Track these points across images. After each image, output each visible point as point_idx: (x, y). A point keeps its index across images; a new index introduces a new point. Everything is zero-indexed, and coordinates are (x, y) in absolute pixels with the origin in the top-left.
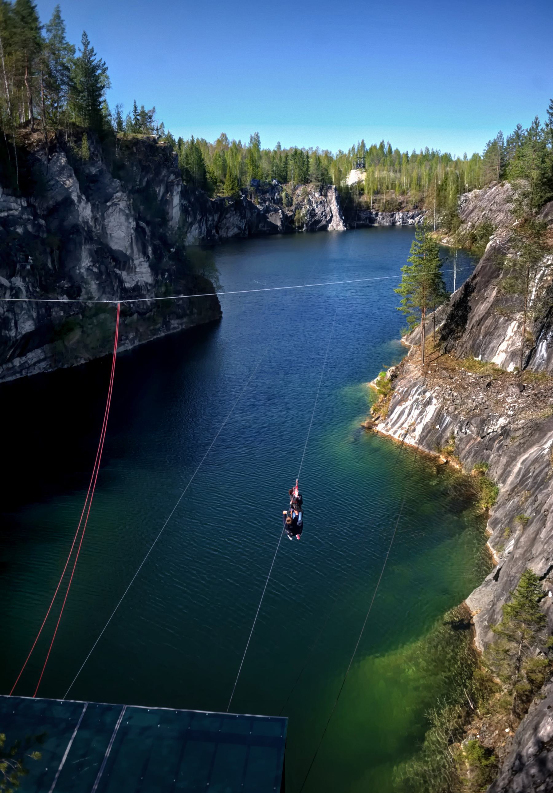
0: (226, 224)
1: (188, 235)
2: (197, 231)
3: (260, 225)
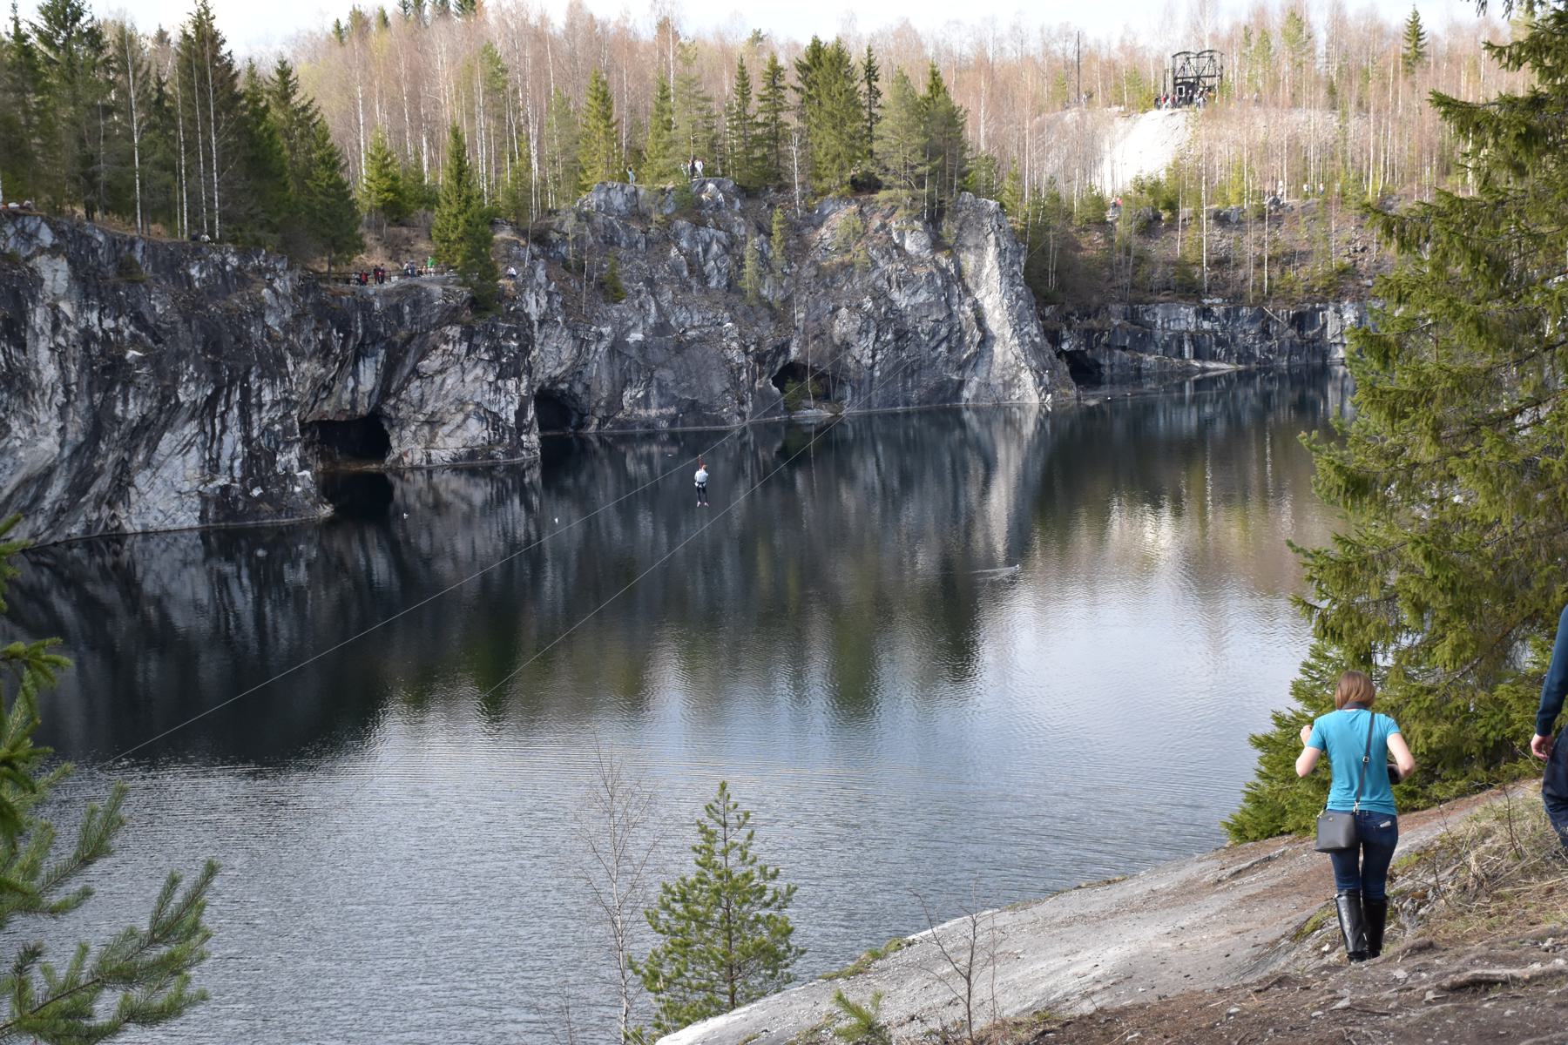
0: (422, 401)
1: (140, 480)
2: (194, 457)
3: (628, 394)
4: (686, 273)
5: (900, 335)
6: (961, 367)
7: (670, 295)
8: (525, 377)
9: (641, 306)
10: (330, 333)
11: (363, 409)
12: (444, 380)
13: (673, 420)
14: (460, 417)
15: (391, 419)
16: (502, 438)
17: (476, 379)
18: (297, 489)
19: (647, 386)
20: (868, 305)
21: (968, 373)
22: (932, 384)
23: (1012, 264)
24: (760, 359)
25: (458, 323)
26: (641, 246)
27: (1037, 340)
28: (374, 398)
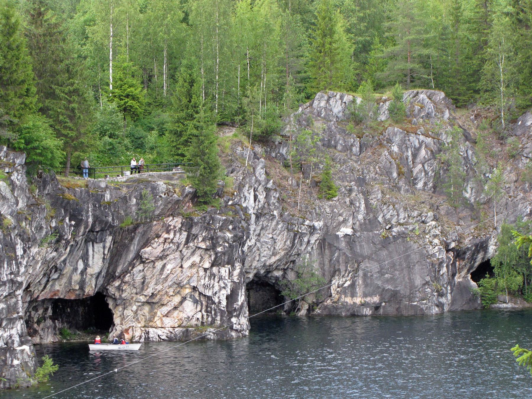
3: (335, 282)
4: (395, 175)
8: (238, 265)
9: (352, 203)
10: (63, 220)
11: (90, 290)
12: (164, 266)
13: (377, 308)
14: (177, 299)
15: (115, 299)
16: (214, 320)
17: (193, 265)
18: (16, 362)
24: (459, 254)
25: (179, 214)
26: (356, 149)
28: (101, 281)
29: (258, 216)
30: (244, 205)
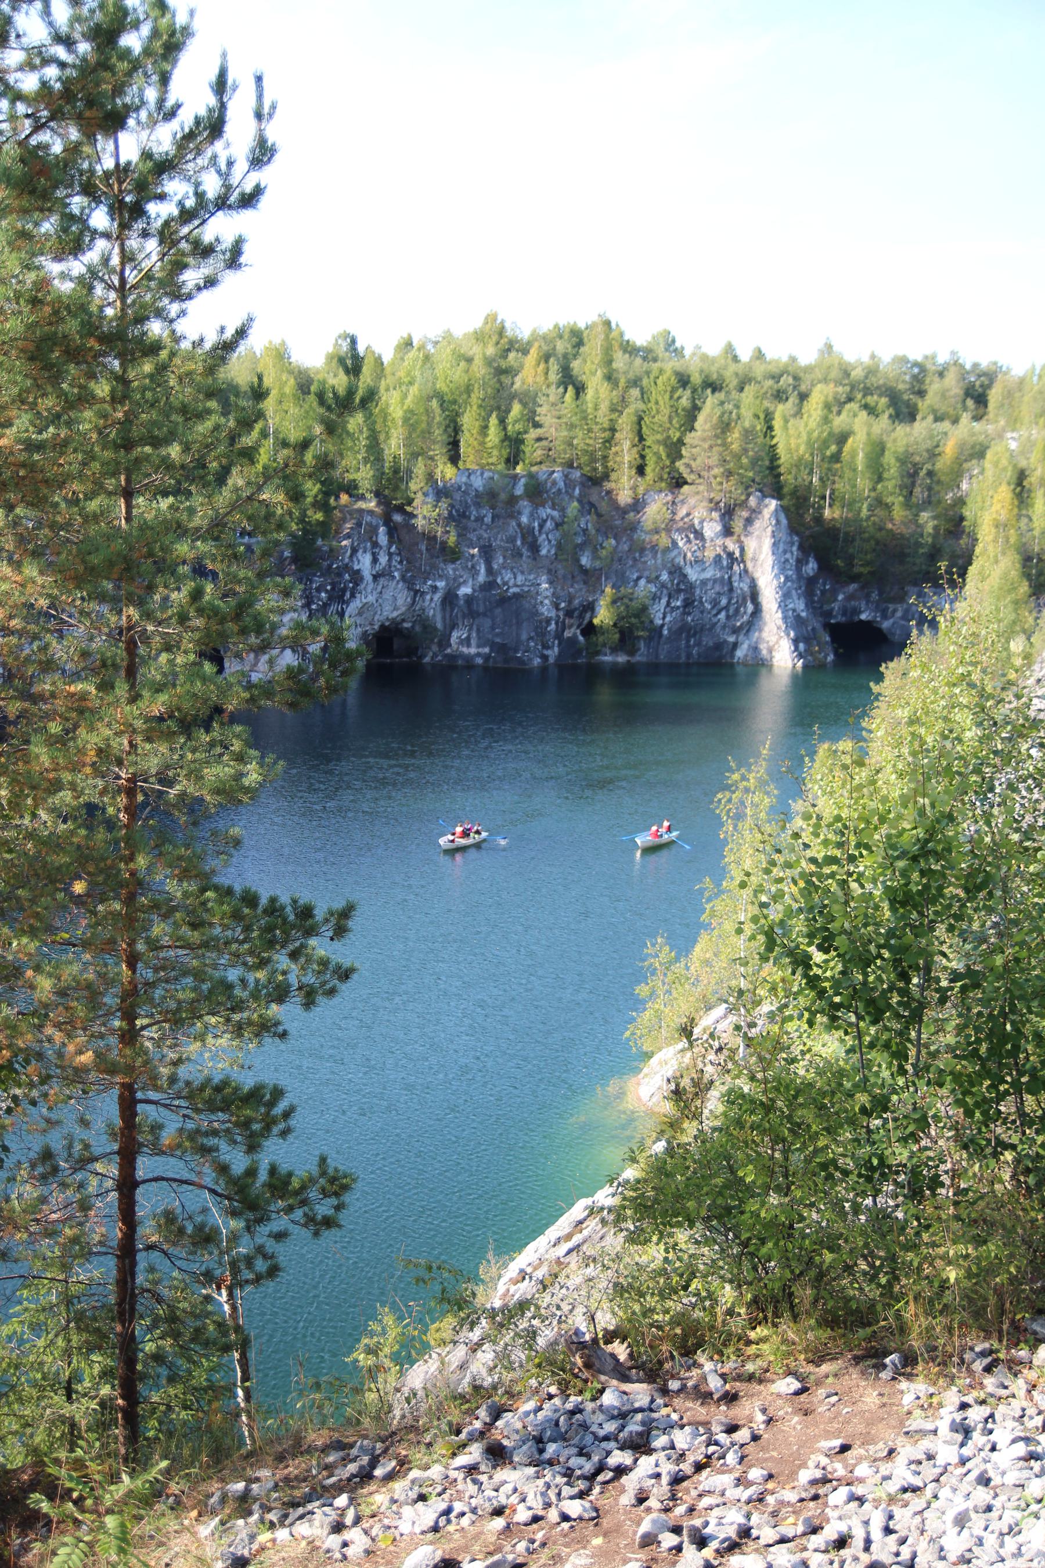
3: (455, 635)
4: (519, 543)
5: (688, 604)
6: (736, 631)
7: (501, 560)
9: (473, 567)
13: (487, 658)
19: (470, 630)
20: (665, 577)
21: (741, 638)
22: (711, 644)
23: (785, 552)
26: (488, 520)
27: (804, 614)
29: (376, 577)
30: (356, 567)
